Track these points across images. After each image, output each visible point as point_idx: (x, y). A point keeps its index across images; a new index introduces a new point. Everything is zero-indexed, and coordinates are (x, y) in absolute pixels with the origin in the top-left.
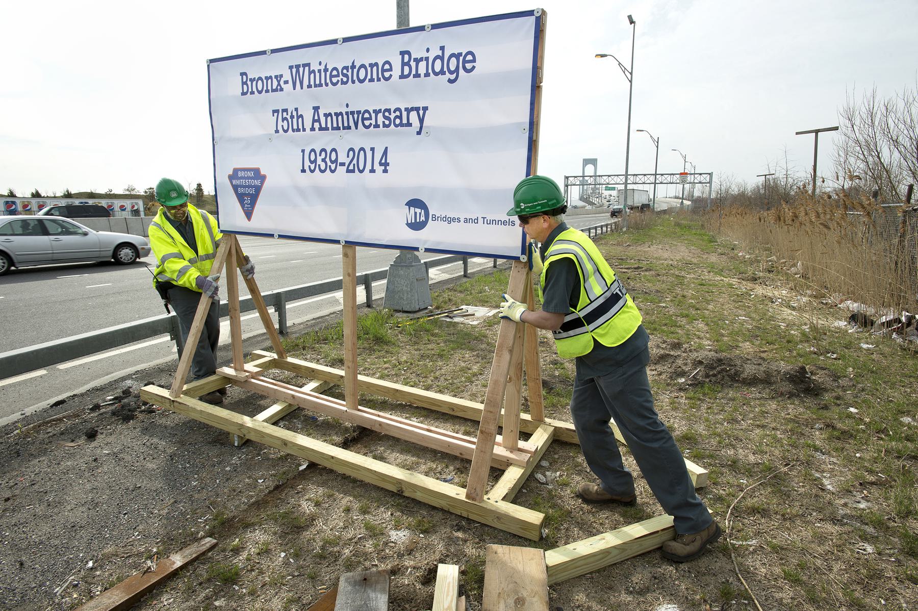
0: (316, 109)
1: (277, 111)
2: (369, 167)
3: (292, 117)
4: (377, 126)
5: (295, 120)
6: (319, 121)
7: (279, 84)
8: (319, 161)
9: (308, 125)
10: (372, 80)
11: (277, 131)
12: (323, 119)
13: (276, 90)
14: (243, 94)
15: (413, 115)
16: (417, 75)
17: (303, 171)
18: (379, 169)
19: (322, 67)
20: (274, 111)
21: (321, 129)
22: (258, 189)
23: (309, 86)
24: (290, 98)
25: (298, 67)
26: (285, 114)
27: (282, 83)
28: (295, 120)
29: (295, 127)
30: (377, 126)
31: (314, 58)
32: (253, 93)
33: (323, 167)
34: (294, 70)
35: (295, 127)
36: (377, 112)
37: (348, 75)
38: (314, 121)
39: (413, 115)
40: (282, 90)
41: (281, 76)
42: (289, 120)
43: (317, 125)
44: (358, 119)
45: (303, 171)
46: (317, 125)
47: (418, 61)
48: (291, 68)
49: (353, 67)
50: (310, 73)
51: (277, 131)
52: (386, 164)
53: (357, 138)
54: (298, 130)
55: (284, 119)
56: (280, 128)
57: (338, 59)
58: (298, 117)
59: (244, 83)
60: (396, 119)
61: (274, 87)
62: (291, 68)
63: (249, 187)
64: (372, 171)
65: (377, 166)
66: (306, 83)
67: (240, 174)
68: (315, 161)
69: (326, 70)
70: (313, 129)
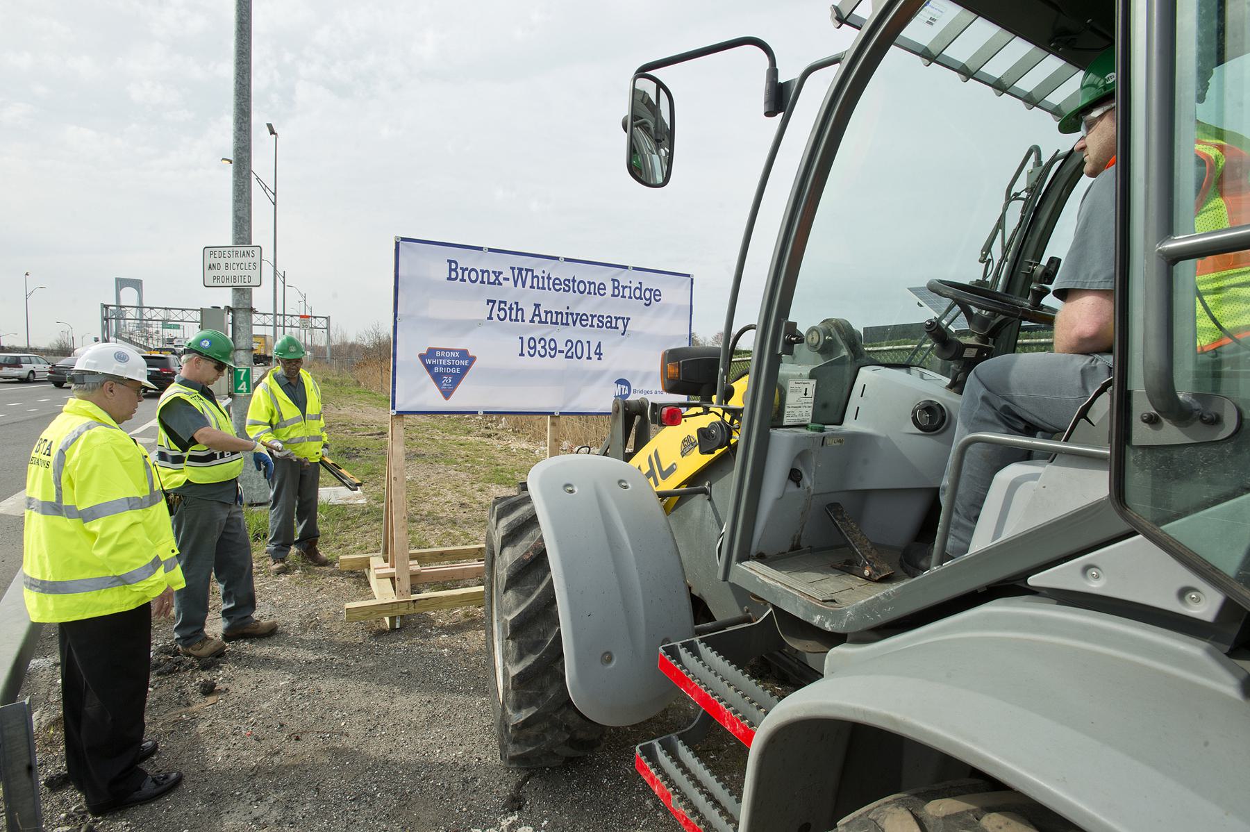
0: (537, 306)
1: (494, 302)
2: (586, 354)
3: (511, 309)
4: (592, 326)
5: (514, 312)
6: (539, 315)
7: (497, 278)
8: (539, 347)
9: (528, 317)
10: (589, 293)
11: (490, 318)
12: (543, 315)
13: (494, 283)
14: (450, 278)
15: (620, 321)
16: (623, 296)
17: (522, 355)
18: (595, 357)
19: (546, 275)
20: (489, 301)
21: (540, 322)
22: (464, 370)
23: (532, 287)
24: (509, 292)
25: (520, 270)
26: (502, 306)
27: (501, 278)
28: (514, 312)
29: (514, 317)
30: (592, 326)
31: (540, 268)
32: (463, 280)
33: (543, 352)
34: (516, 272)
35: (514, 317)
36: (593, 316)
37: (569, 285)
38: (534, 315)
39: (620, 321)
40: (500, 284)
41: (500, 273)
42: (507, 312)
43: (537, 319)
44: (580, 319)
45: (522, 355)
46: (537, 319)
47: (624, 288)
48: (513, 269)
49: (574, 281)
50: (533, 277)
51: (490, 318)
52: (600, 354)
53: (575, 333)
54: (517, 320)
55: (500, 310)
56: (494, 316)
57: (562, 272)
58: (518, 310)
59: (451, 270)
60: (608, 323)
61: (492, 280)
62: (513, 269)
63: (451, 366)
64: (589, 358)
65: (592, 354)
66: (528, 283)
67: (438, 354)
68: (535, 347)
69: (549, 278)
70: (532, 321)
